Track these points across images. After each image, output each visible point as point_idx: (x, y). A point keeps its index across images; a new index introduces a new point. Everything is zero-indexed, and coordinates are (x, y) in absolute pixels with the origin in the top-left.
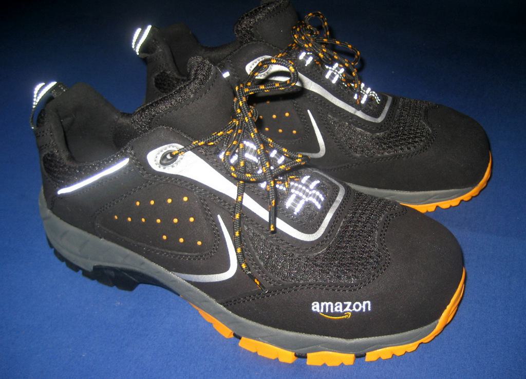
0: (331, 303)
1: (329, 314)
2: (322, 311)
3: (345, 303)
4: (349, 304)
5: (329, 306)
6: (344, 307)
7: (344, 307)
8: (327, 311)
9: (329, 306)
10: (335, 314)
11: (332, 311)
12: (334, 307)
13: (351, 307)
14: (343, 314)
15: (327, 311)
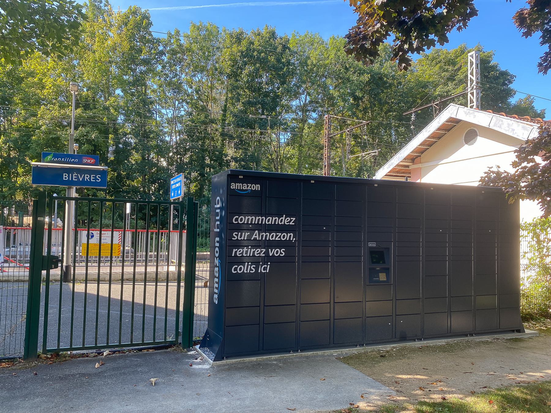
0: (241, 184)
1: (240, 190)
2: (236, 188)
3: (248, 185)
4: (250, 185)
5: (240, 185)
6: (248, 186)
7: (248, 186)
8: (239, 188)
9: (240, 185)
10: (243, 190)
11: (241, 188)
12: (243, 186)
13: (251, 187)
14: (246, 190)
15: (239, 188)
